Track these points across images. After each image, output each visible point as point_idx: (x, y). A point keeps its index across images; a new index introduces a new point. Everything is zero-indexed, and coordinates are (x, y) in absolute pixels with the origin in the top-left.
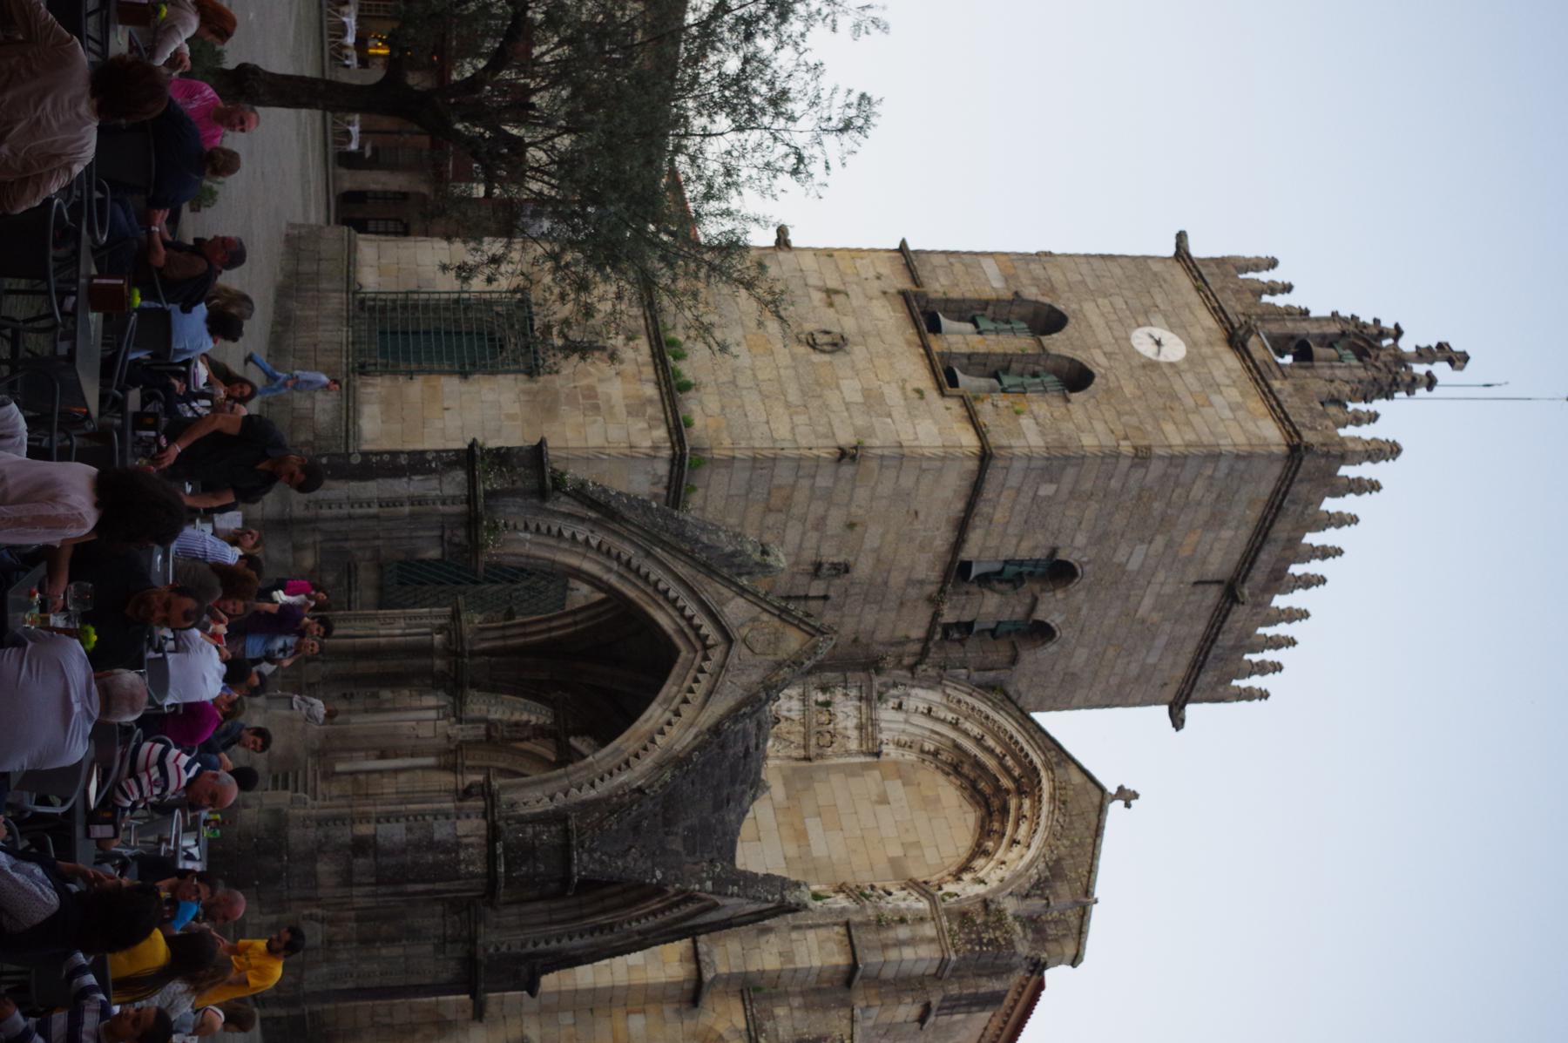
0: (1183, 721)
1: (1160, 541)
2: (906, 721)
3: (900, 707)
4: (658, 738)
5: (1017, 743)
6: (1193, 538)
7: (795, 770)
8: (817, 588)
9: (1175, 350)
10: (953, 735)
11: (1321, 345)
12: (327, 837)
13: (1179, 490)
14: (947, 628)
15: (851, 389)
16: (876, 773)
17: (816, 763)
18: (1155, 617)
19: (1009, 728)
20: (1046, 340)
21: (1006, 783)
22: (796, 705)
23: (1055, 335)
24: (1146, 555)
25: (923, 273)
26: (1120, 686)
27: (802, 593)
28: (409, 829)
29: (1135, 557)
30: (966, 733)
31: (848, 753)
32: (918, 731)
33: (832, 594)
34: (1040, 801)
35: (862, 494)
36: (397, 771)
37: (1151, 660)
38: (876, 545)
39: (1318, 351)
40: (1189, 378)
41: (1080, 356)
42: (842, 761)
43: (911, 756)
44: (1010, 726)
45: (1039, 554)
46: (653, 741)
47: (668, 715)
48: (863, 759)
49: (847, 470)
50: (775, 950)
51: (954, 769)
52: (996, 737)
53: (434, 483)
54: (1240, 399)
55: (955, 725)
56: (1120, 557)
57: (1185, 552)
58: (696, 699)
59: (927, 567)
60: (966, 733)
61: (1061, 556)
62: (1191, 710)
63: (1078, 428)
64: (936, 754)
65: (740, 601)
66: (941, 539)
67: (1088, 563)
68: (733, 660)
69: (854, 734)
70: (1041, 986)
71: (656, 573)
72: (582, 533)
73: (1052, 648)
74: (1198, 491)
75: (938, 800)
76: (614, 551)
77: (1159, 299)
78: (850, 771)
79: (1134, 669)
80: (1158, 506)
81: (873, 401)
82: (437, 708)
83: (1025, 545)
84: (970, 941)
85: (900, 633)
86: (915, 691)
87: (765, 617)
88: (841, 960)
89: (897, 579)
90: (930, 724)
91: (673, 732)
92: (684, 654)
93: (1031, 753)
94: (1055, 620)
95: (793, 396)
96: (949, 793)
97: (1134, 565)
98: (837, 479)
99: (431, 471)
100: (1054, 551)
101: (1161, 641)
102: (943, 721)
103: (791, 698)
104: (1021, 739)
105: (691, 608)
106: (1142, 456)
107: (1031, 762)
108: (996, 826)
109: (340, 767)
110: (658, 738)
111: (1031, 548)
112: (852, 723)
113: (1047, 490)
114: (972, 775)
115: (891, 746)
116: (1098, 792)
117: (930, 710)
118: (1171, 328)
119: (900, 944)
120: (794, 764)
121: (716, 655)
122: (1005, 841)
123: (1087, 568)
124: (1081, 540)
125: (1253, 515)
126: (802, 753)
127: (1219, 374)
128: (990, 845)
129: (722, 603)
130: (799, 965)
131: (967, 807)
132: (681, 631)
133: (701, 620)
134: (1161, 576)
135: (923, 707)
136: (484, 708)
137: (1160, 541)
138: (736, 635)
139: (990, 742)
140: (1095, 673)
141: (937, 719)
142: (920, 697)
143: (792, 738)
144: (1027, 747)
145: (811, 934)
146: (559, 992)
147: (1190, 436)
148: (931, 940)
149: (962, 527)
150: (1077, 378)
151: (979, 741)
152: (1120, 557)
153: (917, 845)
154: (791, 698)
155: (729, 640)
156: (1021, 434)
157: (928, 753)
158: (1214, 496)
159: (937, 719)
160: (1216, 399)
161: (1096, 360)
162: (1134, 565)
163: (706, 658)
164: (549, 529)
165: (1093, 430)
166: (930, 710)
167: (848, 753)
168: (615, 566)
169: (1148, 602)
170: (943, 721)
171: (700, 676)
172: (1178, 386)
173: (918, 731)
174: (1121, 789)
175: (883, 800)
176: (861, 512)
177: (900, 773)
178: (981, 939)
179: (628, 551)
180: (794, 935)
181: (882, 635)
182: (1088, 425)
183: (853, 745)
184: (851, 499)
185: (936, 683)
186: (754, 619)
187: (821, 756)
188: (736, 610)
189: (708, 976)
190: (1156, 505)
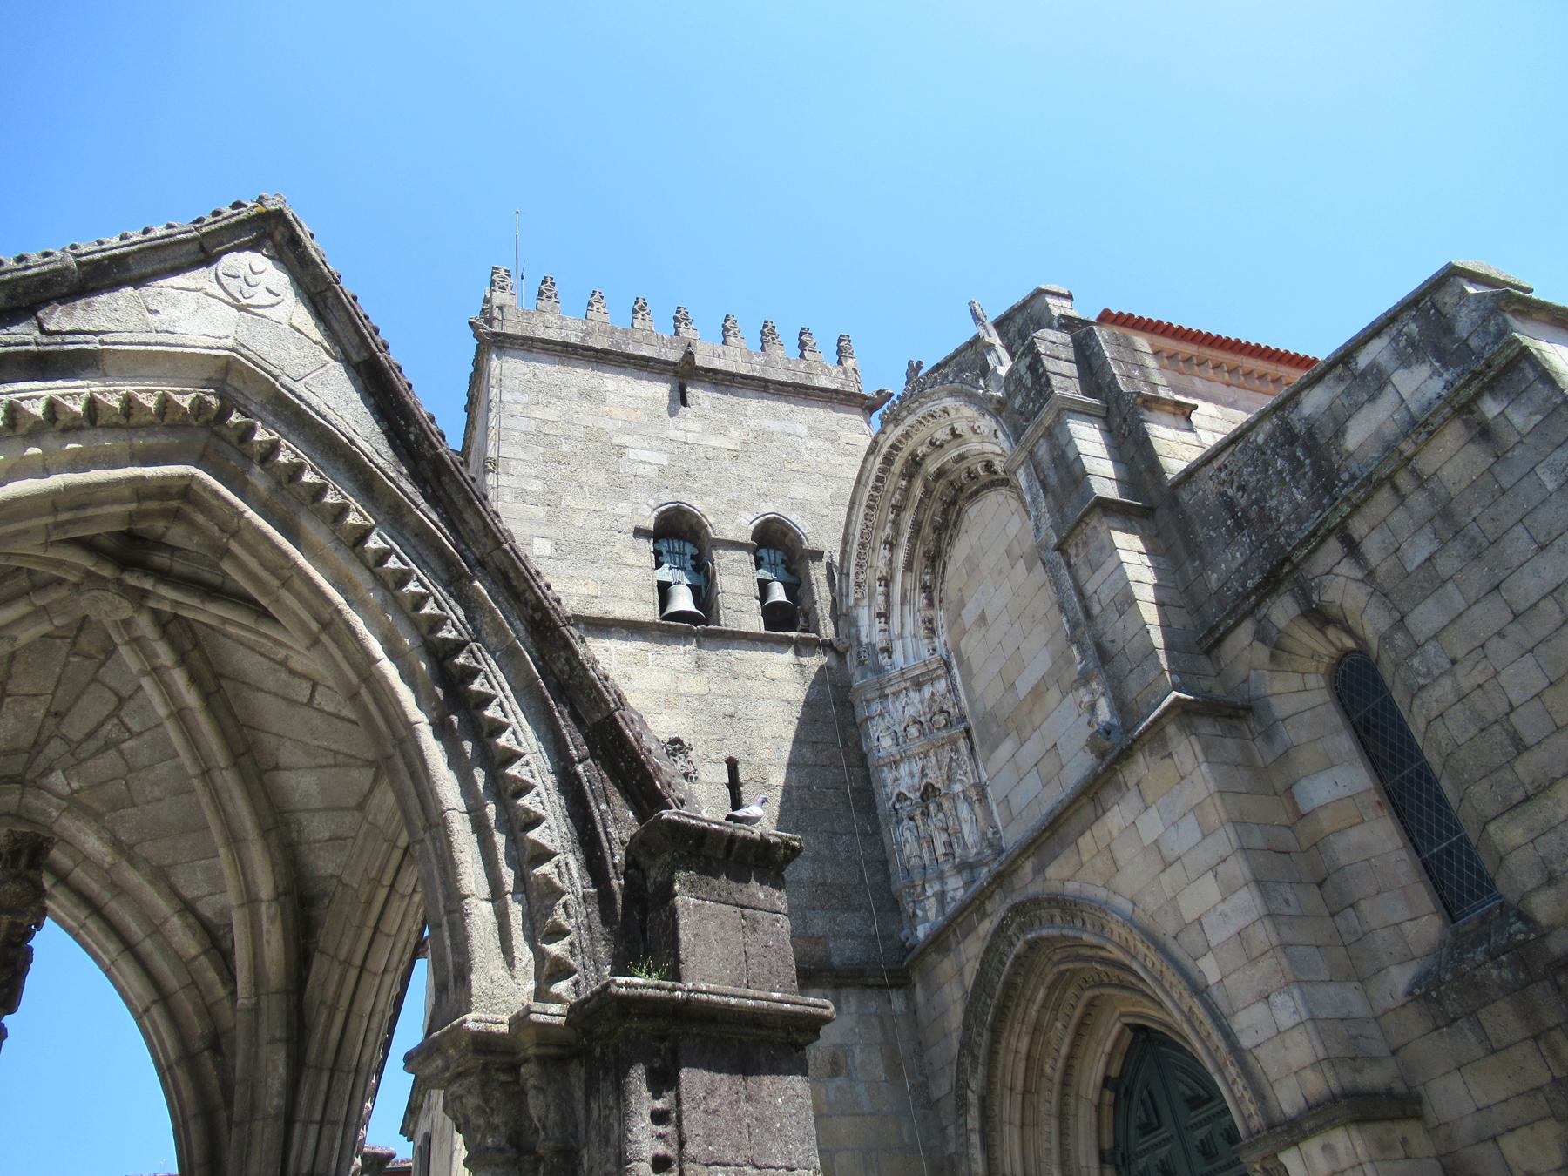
2: (901, 637)
3: (888, 651)
5: (872, 498)
6: (618, 413)
7: (982, 742)
10: (898, 577)
16: (962, 644)
19: (861, 515)
21: (918, 489)
31: (952, 689)
33: (725, 754)
34: (907, 435)
45: (647, 546)
48: (955, 671)
50: (1120, 624)
51: (935, 559)
55: (887, 581)
61: (650, 524)
64: (927, 589)
69: (927, 690)
74: (550, 414)
75: (968, 558)
78: (968, 676)
83: (630, 558)
86: (864, 640)
89: (694, 684)
93: (873, 477)
96: (960, 551)
97: (663, 459)
100: (639, 533)
102: (887, 596)
103: (896, 779)
107: (882, 471)
112: (914, 696)
117: (879, 615)
120: (977, 748)
122: (964, 449)
123: (667, 497)
124: (624, 508)
131: (965, 525)
139: (888, 529)
140: (828, 478)
144: (871, 484)
145: (1089, 588)
151: (891, 545)
152: (651, 472)
153: (1008, 552)
158: (554, 400)
166: (879, 615)
167: (952, 689)
169: (716, 441)
170: (887, 596)
173: (909, 621)
175: (982, 618)
177: (955, 619)
180: (1096, 610)
183: (942, 686)
187: (962, 718)
190: (565, 448)
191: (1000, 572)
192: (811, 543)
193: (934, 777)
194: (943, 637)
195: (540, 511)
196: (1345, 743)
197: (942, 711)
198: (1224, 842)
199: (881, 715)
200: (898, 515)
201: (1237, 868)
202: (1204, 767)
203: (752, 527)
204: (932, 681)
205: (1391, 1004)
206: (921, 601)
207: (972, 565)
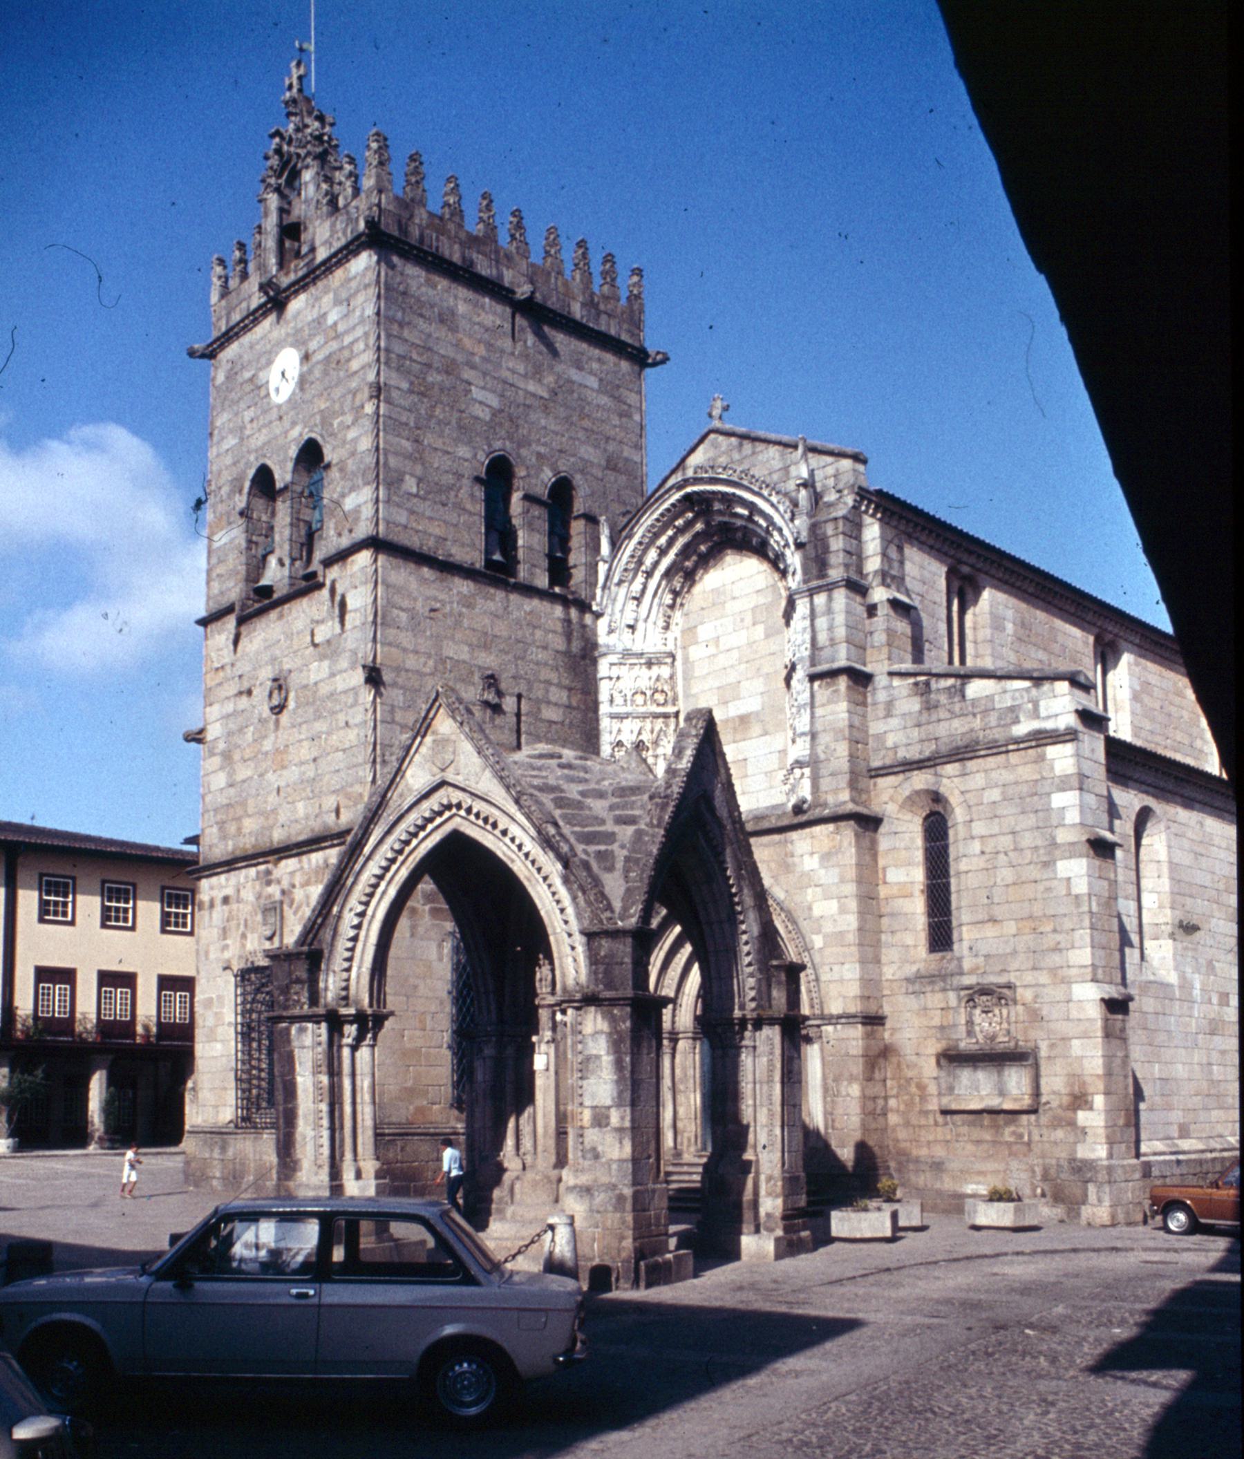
0: (658, 353)
1: (467, 374)
2: (646, 620)
4: (525, 849)
6: (467, 342)
8: (509, 704)
9: (288, 360)
11: (288, 212)
13: (415, 356)
14: (552, 583)
15: (318, 671)
18: (550, 379)
19: (649, 522)
20: (279, 485)
21: (699, 526)
23: (277, 476)
24: (483, 388)
25: (224, 602)
26: (621, 416)
27: (514, 719)
29: (483, 401)
30: (656, 564)
33: (516, 691)
35: (411, 662)
37: (593, 382)
38: (466, 649)
39: (293, 218)
40: (313, 345)
41: (293, 452)
43: (677, 616)
45: (480, 493)
46: (527, 855)
47: (507, 840)
49: (387, 676)
52: (657, 536)
54: (331, 295)
55: (649, 574)
56: (485, 415)
57: (481, 350)
59: (493, 603)
60: (656, 564)
62: (652, 342)
63: (353, 454)
64: (676, 594)
65: (409, 773)
66: (463, 586)
67: (490, 446)
68: (459, 780)
69: (655, 670)
70: (879, 493)
73: (578, 480)
76: (368, 890)
77: (247, 375)
79: (604, 400)
80: (434, 377)
81: (326, 650)
83: (469, 506)
85: (559, 627)
88: (843, 682)
92: (456, 823)
94: (548, 476)
95: (321, 726)
96: (712, 580)
97: (494, 402)
98: (395, 684)
100: (477, 479)
101: (574, 375)
106: (378, 391)
107: (678, 501)
108: (739, 535)
110: (525, 849)
111: (473, 501)
113: (410, 485)
114: (694, 558)
117: (634, 598)
118: (270, 363)
119: (831, 629)
122: (751, 526)
123: (498, 444)
125: (443, 283)
126: (673, 720)
127: (311, 315)
128: (754, 541)
130: (846, 723)
133: (426, 808)
134: (506, 374)
135: (632, 605)
137: (467, 374)
139: (663, 540)
141: (643, 591)
143: (657, 729)
146: (861, 945)
147: (361, 345)
148: (830, 599)
149: (447, 568)
150: (311, 456)
151: (663, 552)
152: (485, 415)
155: (443, 784)
156: (357, 510)
157: (674, 600)
159: (643, 591)
160: (330, 321)
161: (297, 435)
162: (494, 402)
163: (459, 806)
164: (348, 950)
165: (355, 440)
166: (634, 598)
169: (532, 387)
171: (475, 810)
172: (319, 356)
176: (431, 663)
181: (559, 643)
182: (350, 444)
183: (665, 671)
184: (418, 672)
187: (675, 700)
188: (417, 777)
189: (850, 807)
191: (742, 620)
193: (646, 737)
194: (675, 631)
195: (407, 445)
196: (919, 856)
197: (663, 691)
198: (850, 888)
199: (618, 678)
201: (853, 905)
202: (853, 850)
204: (660, 663)
206: (668, 599)
207: (718, 599)
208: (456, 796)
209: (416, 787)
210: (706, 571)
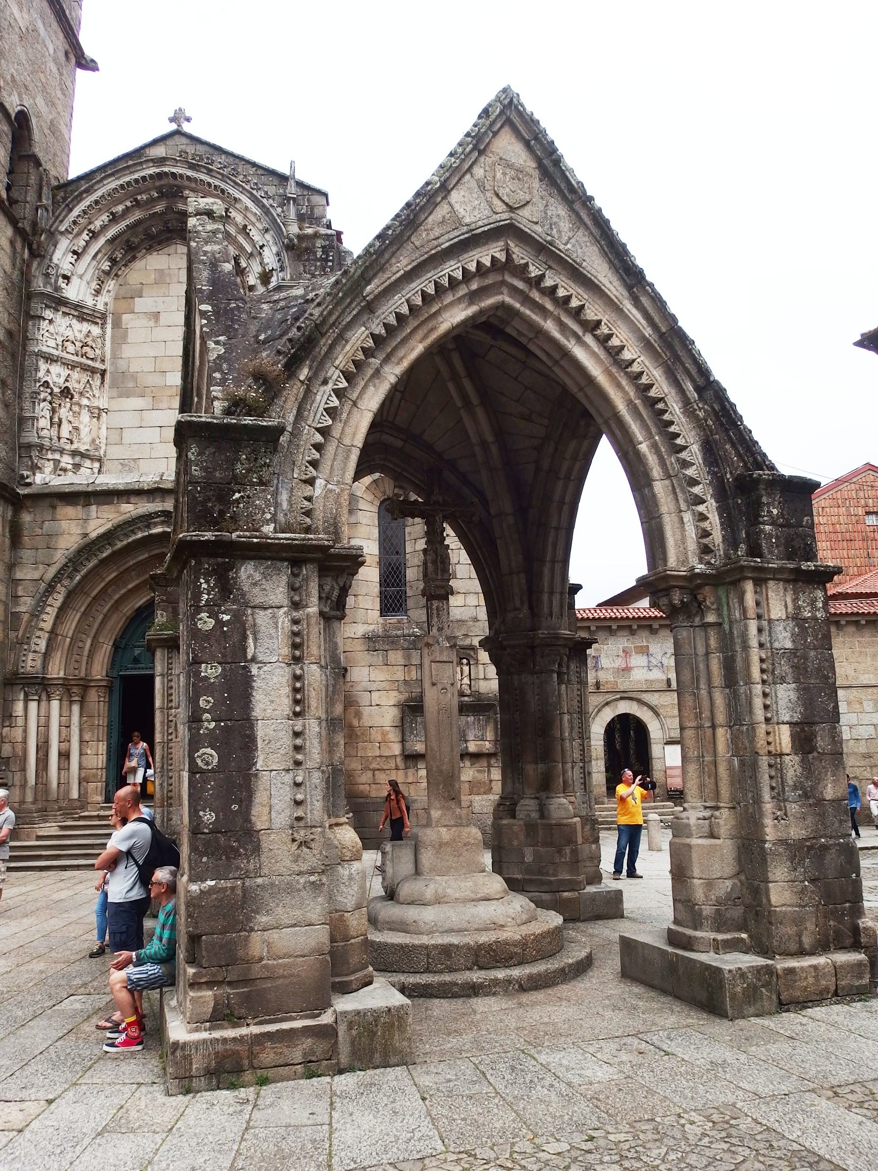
0: (93, 61)
2: (81, 277)
5: (129, 183)
10: (102, 241)
12: (795, 788)
16: (124, 317)
17: (107, 366)
19: (113, 185)
21: (159, 208)
22: (55, 369)
28: (783, 680)
30: (104, 228)
32: (91, 271)
36: (81, 741)
42: (108, 343)
43: (111, 285)
44: (112, 184)
48: (109, 326)
53: (262, 618)
55: (94, 235)
58: (578, 297)
60: (104, 228)
64: (113, 261)
65: (455, 196)
69: (86, 327)
71: (398, 303)
72: (324, 396)
75: (161, 272)
78: (121, 337)
82: (26, 701)
84: (323, 268)
86: (55, 260)
87: (479, 172)
90: (87, 258)
91: (621, 336)
93: (142, 174)
99: (238, 619)
104: (127, 179)
105: (452, 268)
107: (151, 176)
109: (75, 795)
115: (99, 299)
116: (177, 138)
117: (75, 252)
121: (521, 256)
129: (458, 222)
132: (473, 297)
135: (71, 258)
136: (31, 656)
138: (505, 216)
139: (120, 208)
141: (85, 248)
142: (61, 256)
143: (84, 381)
144: (136, 176)
151: (114, 219)
154: (48, 371)
159: (85, 248)
166: (75, 252)
167: (103, 336)
168: (375, 362)
174: (172, 120)
175: (156, 316)
177: (128, 297)
178: (321, 259)
179: (359, 337)
183: (96, 330)
185: (53, 236)
186: (482, 187)
192: (38, 150)
200: (132, 206)
203: (16, 110)
205: (353, 636)
208: (521, 256)
209: (467, 220)
210: (150, 249)
